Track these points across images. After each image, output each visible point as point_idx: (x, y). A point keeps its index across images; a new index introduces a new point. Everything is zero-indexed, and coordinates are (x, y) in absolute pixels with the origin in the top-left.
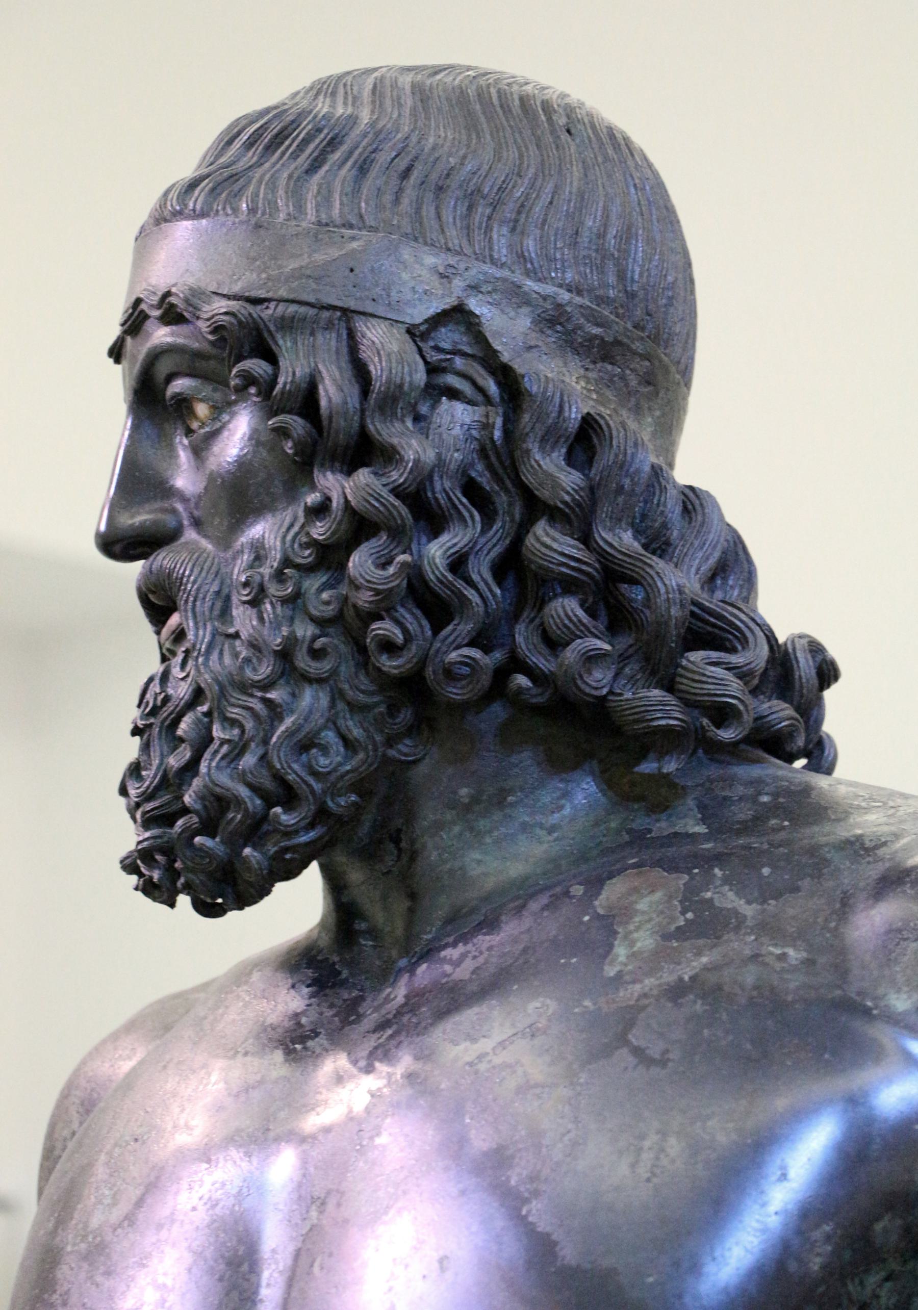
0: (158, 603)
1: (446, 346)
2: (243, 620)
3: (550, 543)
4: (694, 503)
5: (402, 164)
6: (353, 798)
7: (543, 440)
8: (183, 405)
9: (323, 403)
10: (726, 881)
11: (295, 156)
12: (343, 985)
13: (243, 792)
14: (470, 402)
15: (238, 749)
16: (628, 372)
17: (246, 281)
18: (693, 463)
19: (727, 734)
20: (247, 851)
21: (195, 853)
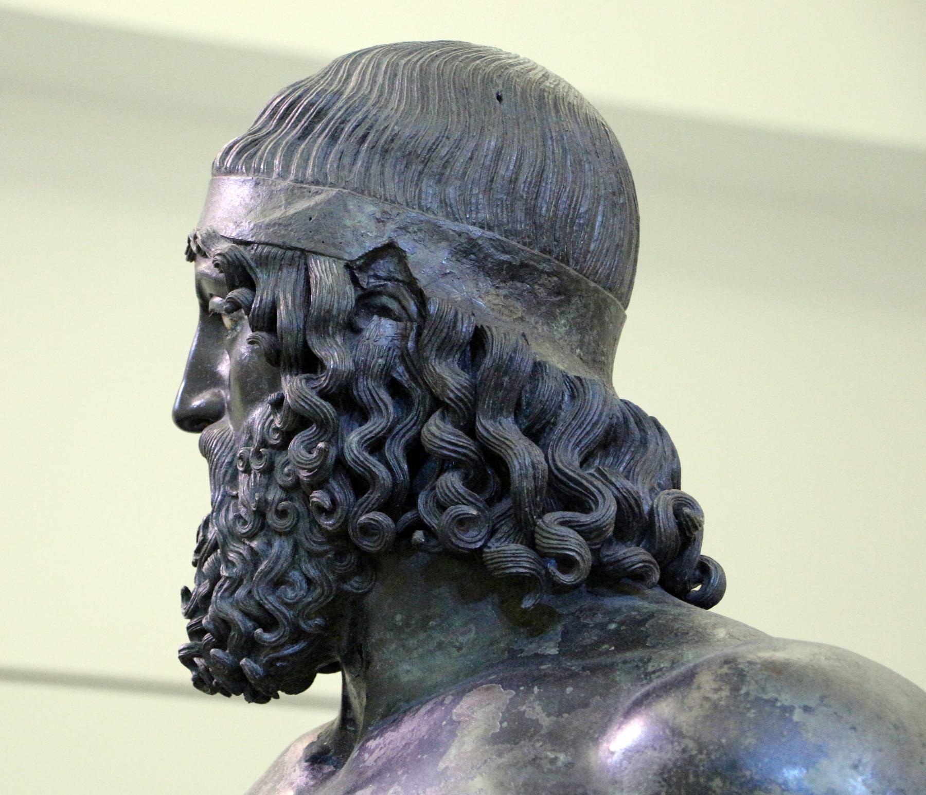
1: (382, 273)
3: (439, 431)
5: (360, 132)
6: (318, 621)
7: (440, 349)
9: (278, 324)
10: (539, 698)
11: (295, 126)
13: (236, 616)
14: (397, 319)
16: (537, 287)
19: (567, 579)
20: (243, 661)
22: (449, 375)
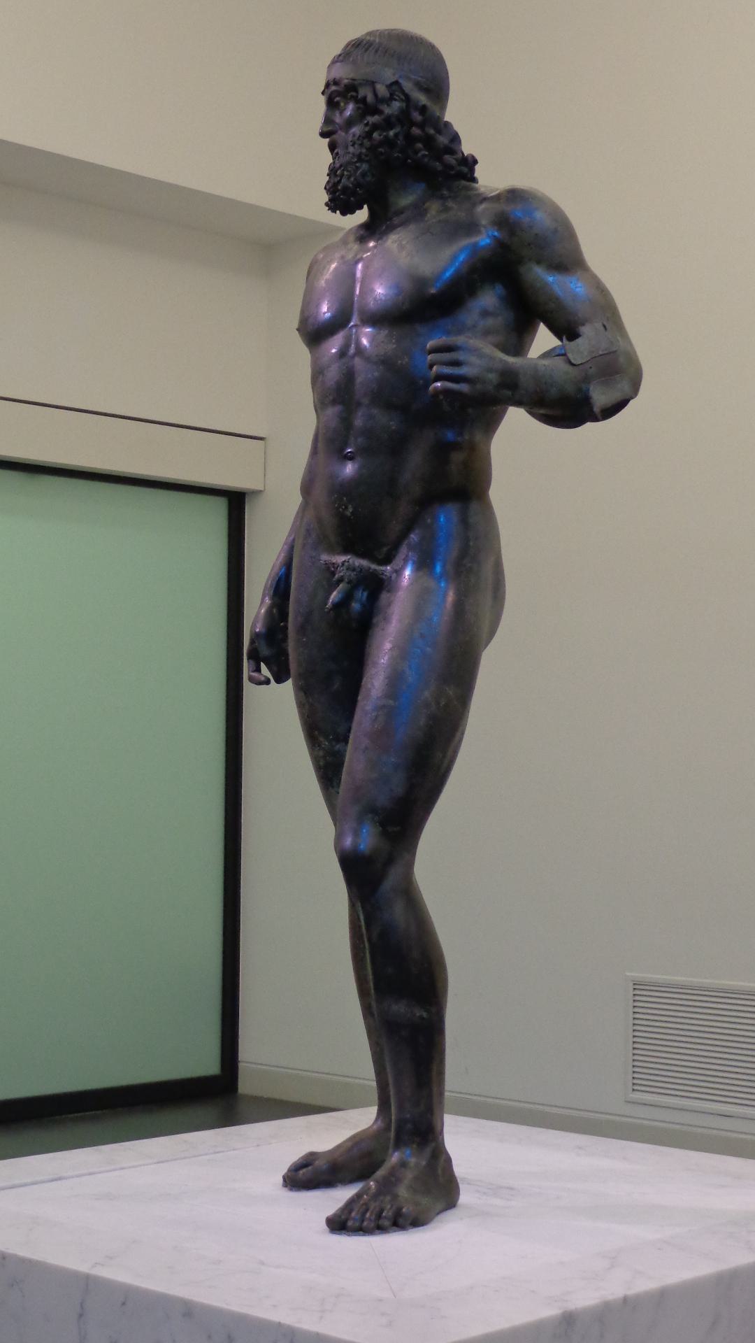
0: (332, 147)
2: (351, 149)
3: (416, 131)
4: (447, 124)
8: (338, 103)
12: (370, 230)
15: (349, 177)
17: (351, 76)
18: (448, 117)
21: (341, 201)
22: (417, 117)
